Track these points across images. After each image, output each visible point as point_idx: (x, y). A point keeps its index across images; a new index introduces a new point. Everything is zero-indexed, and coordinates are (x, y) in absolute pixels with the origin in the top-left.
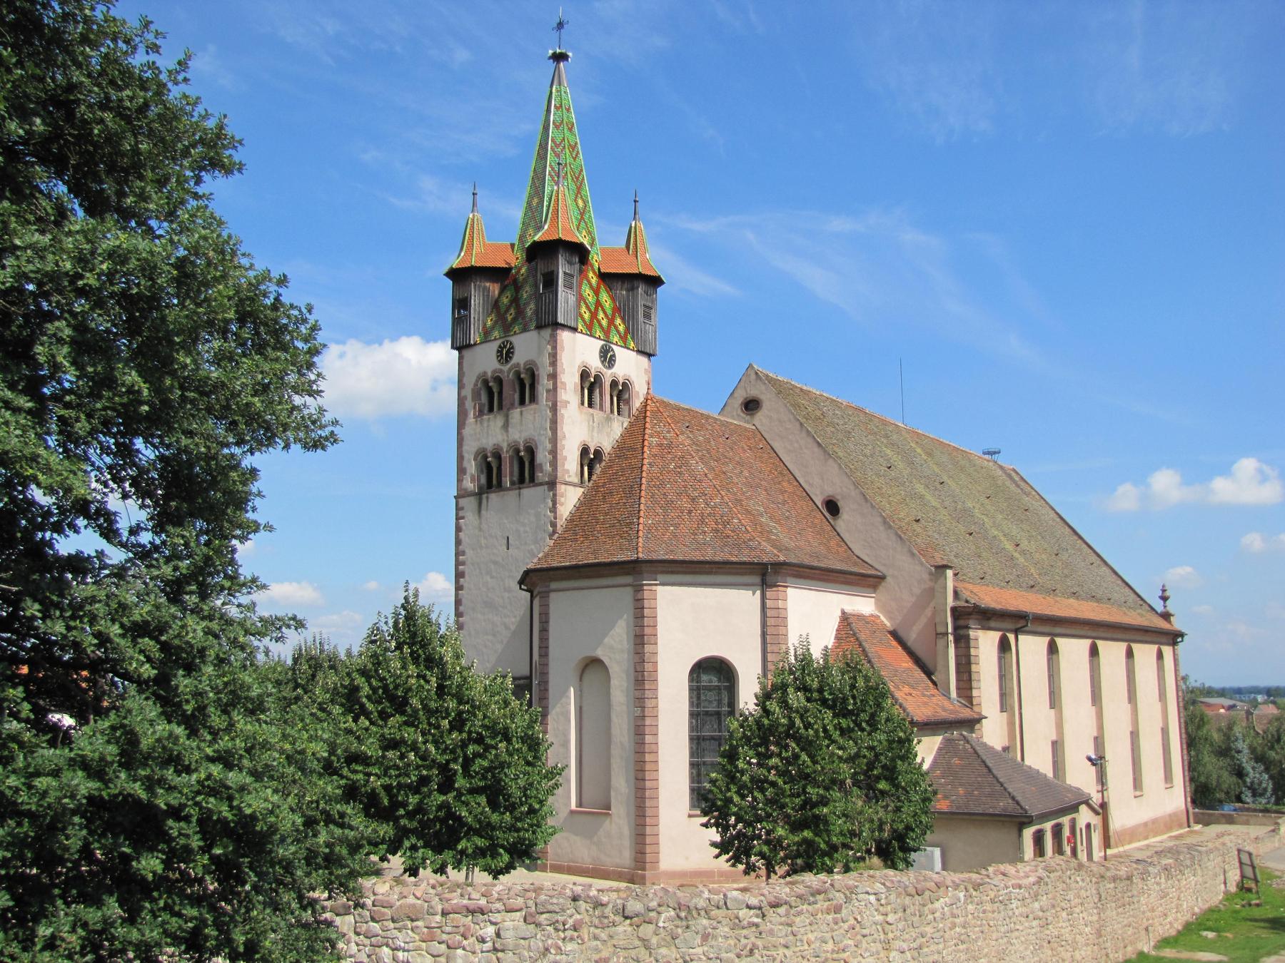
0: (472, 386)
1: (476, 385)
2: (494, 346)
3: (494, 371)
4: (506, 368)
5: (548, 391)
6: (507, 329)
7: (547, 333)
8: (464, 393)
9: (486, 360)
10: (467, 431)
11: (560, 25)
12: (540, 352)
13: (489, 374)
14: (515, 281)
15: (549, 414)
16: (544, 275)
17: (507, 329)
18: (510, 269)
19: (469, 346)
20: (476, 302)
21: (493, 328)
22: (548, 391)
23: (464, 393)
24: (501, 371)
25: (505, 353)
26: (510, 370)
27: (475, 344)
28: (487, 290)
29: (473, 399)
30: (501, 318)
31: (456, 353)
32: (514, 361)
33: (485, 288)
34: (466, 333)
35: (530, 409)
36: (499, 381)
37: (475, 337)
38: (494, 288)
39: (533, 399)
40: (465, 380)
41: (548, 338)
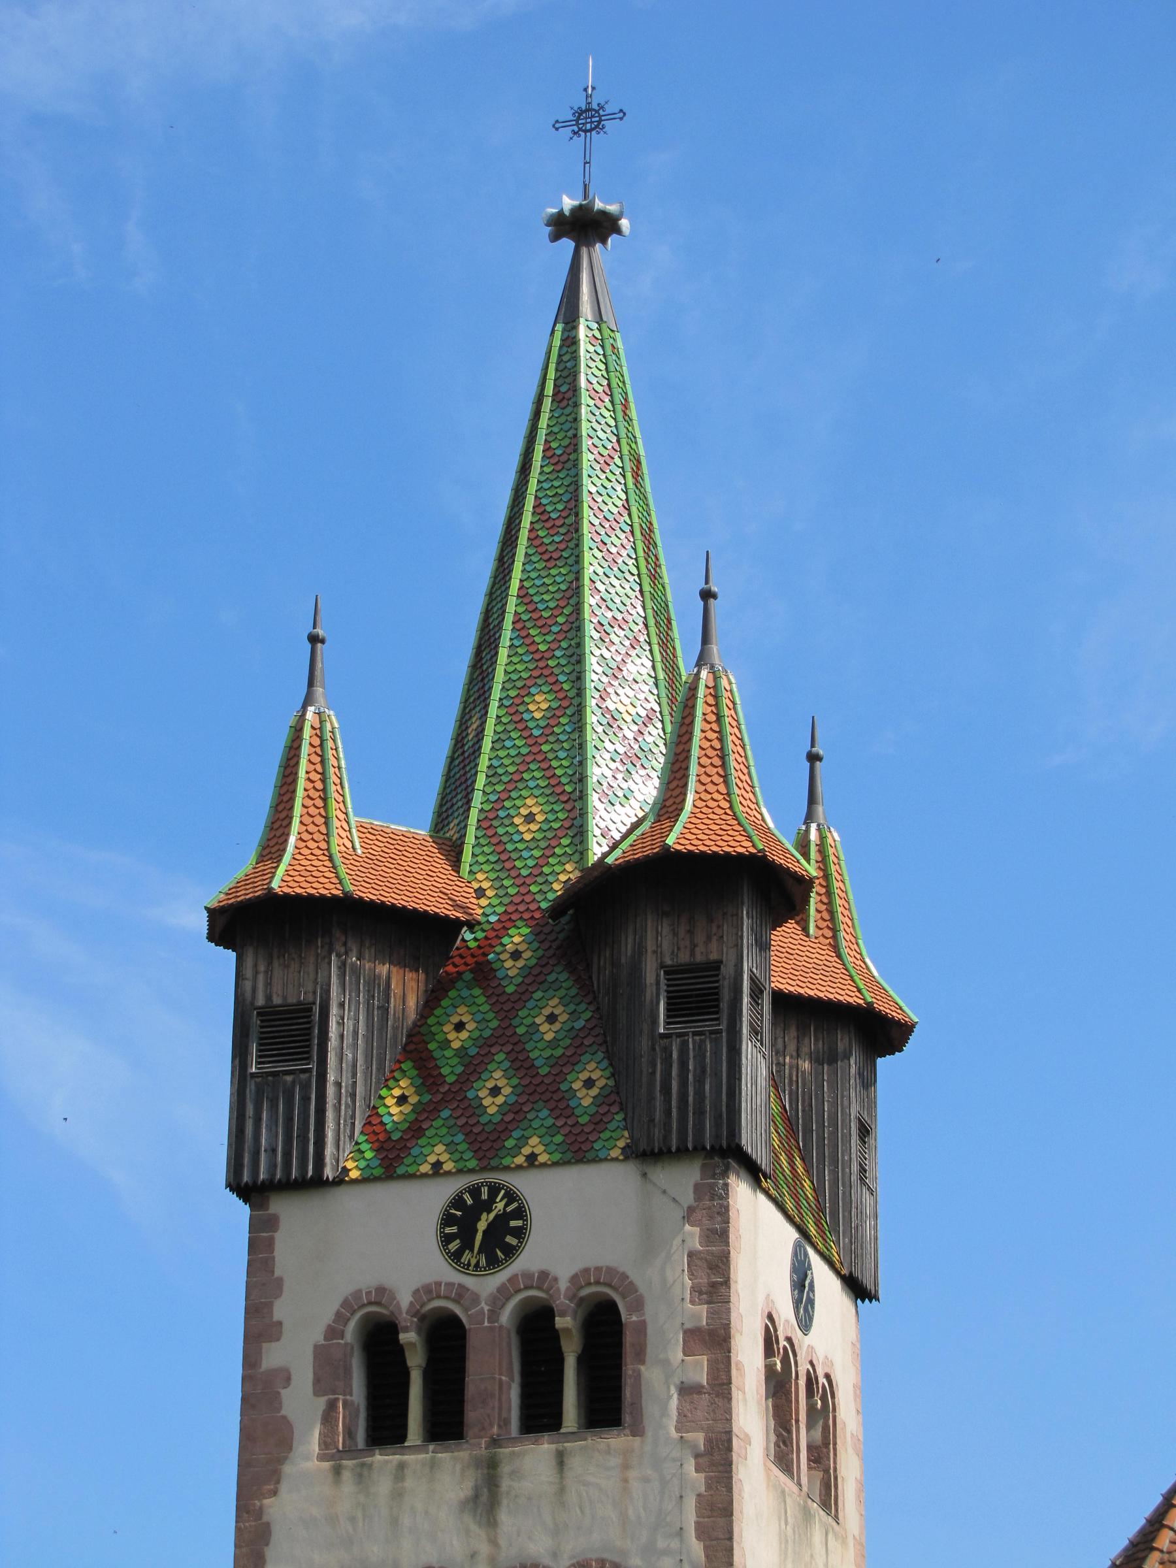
0: (317, 1335)
1: (333, 1332)
2: (434, 1198)
3: (429, 1291)
4: (487, 1285)
5: (687, 1391)
6: (487, 1143)
7: (681, 1180)
8: (273, 1357)
9: (383, 1243)
10: (286, 1507)
11: (588, 119)
12: (650, 1243)
13: (405, 1299)
14: (484, 972)
15: (696, 1479)
16: (671, 972)
17: (487, 1143)
18: (453, 926)
19: (318, 1183)
20: (345, 1031)
21: (415, 1129)
22: (687, 1391)
23: (273, 1357)
24: (461, 1293)
25: (483, 1229)
26: (504, 1293)
27: (340, 1181)
28: (380, 991)
29: (320, 1385)
30: (442, 1096)
31: (242, 1211)
32: (528, 1260)
33: (373, 980)
34: (305, 1131)
35: (598, 1459)
36: (447, 1335)
37: (345, 1154)
38: (406, 989)
39: (607, 1408)
40: (281, 1310)
41: (688, 1198)
